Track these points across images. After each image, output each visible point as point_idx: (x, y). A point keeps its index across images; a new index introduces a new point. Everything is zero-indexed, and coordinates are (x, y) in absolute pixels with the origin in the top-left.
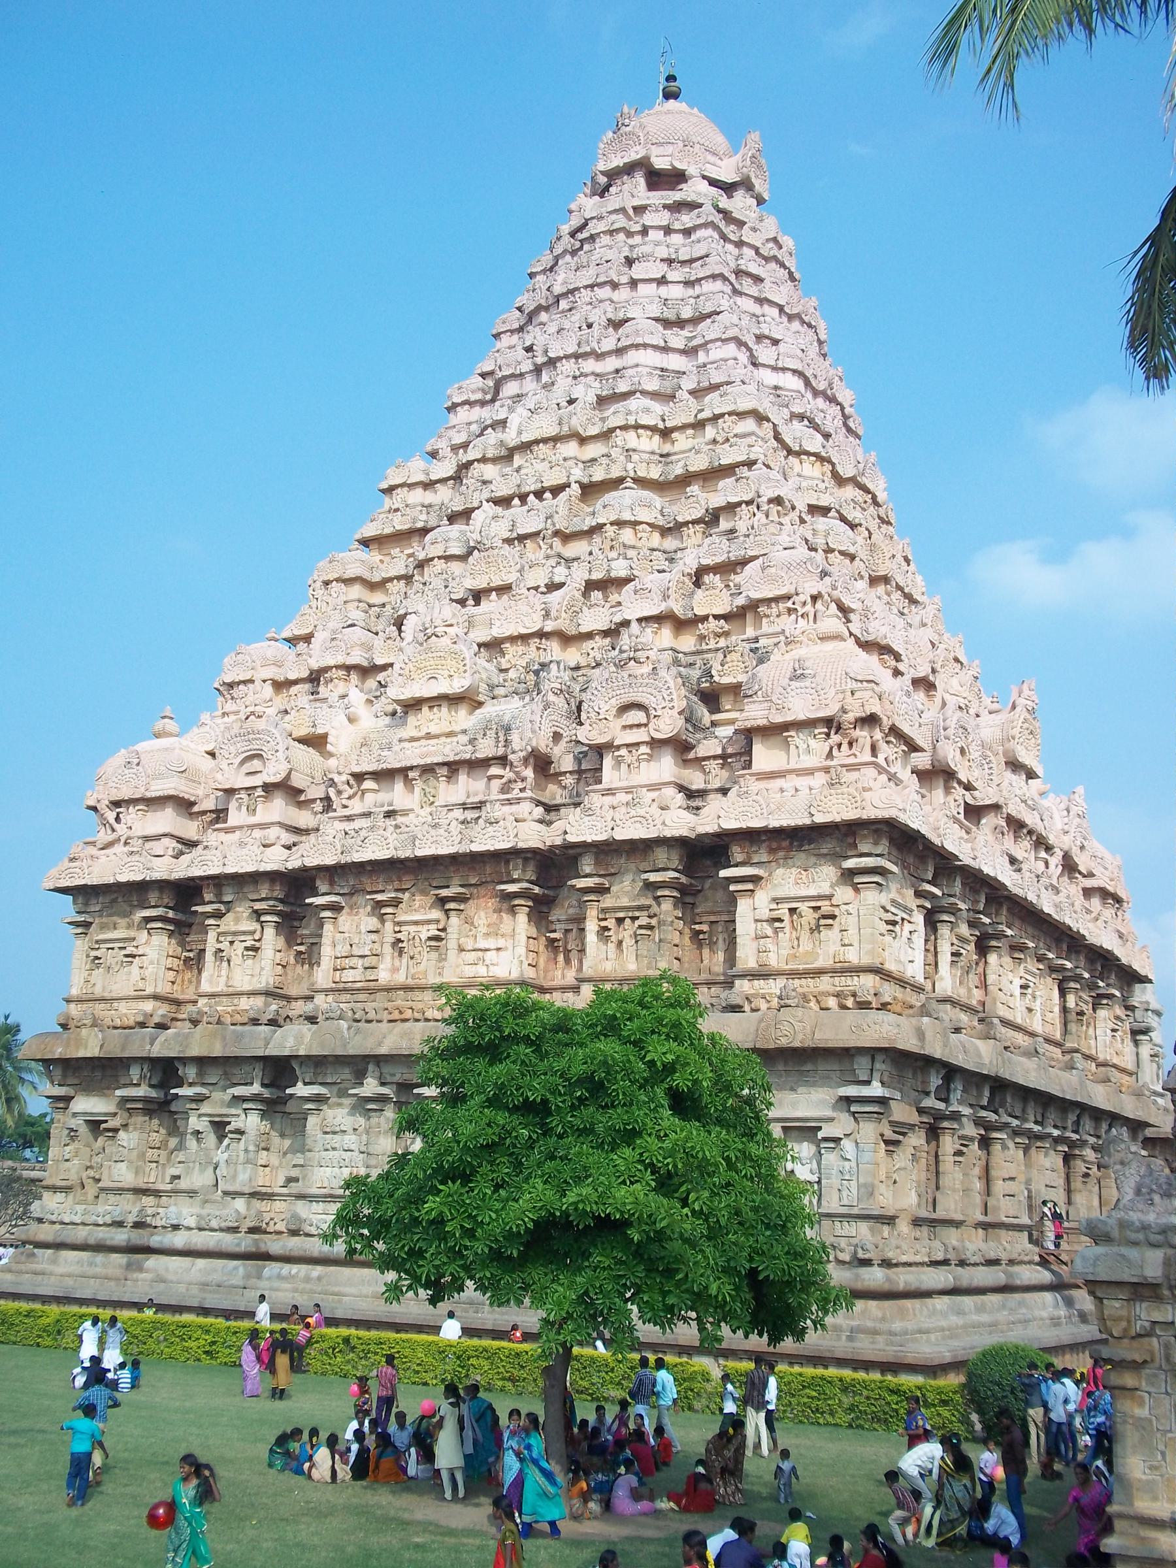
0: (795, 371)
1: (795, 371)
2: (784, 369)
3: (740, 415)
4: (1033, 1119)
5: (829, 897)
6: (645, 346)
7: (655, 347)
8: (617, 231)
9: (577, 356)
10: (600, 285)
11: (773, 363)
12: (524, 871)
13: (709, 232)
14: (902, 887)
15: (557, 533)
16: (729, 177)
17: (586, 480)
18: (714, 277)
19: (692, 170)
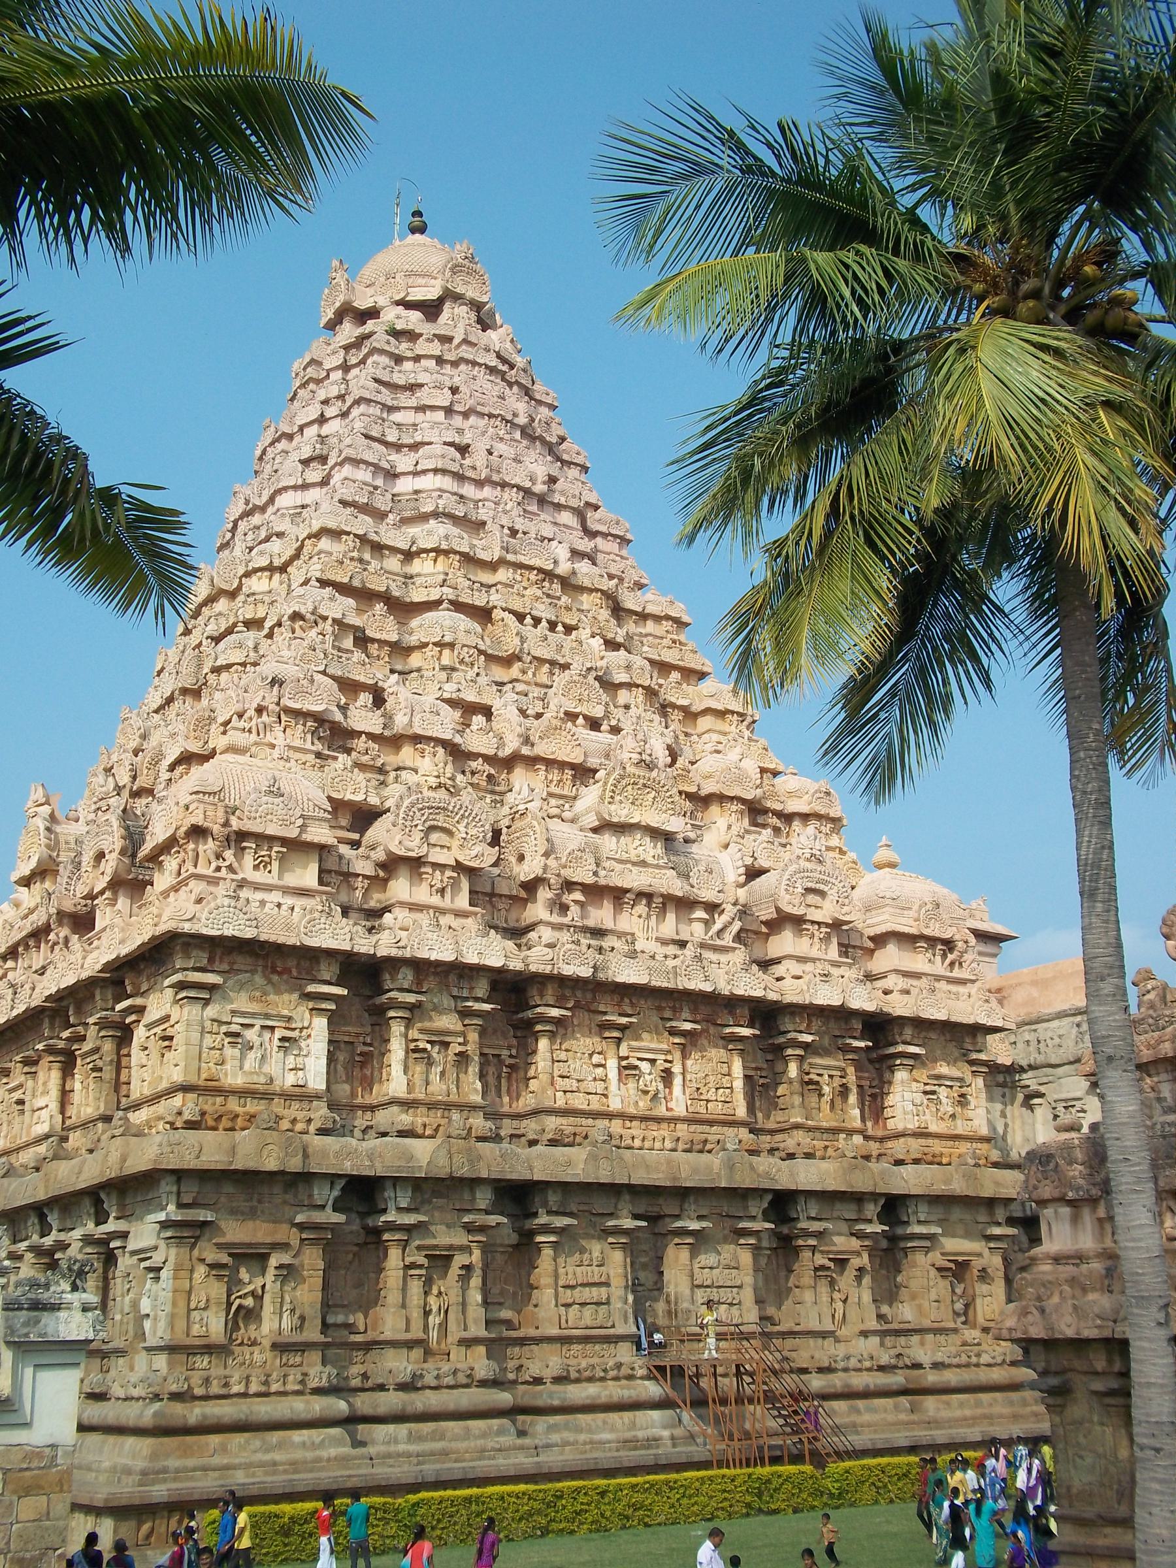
0: (436, 471)
1: (436, 471)
2: (424, 472)
3: (316, 535)
4: (625, 1212)
5: (167, 1018)
6: (285, 489)
7: (295, 488)
8: (307, 383)
9: (247, 514)
10: (278, 440)
11: (411, 469)
12: (52, 1028)
13: (376, 357)
14: (265, 994)
15: (185, 691)
16: (431, 292)
17: (216, 634)
18: (358, 402)
19: (382, 301)
